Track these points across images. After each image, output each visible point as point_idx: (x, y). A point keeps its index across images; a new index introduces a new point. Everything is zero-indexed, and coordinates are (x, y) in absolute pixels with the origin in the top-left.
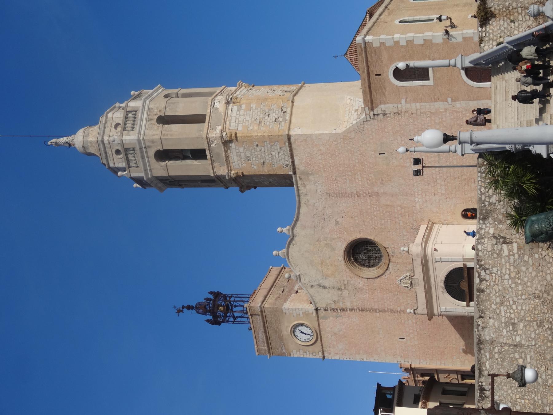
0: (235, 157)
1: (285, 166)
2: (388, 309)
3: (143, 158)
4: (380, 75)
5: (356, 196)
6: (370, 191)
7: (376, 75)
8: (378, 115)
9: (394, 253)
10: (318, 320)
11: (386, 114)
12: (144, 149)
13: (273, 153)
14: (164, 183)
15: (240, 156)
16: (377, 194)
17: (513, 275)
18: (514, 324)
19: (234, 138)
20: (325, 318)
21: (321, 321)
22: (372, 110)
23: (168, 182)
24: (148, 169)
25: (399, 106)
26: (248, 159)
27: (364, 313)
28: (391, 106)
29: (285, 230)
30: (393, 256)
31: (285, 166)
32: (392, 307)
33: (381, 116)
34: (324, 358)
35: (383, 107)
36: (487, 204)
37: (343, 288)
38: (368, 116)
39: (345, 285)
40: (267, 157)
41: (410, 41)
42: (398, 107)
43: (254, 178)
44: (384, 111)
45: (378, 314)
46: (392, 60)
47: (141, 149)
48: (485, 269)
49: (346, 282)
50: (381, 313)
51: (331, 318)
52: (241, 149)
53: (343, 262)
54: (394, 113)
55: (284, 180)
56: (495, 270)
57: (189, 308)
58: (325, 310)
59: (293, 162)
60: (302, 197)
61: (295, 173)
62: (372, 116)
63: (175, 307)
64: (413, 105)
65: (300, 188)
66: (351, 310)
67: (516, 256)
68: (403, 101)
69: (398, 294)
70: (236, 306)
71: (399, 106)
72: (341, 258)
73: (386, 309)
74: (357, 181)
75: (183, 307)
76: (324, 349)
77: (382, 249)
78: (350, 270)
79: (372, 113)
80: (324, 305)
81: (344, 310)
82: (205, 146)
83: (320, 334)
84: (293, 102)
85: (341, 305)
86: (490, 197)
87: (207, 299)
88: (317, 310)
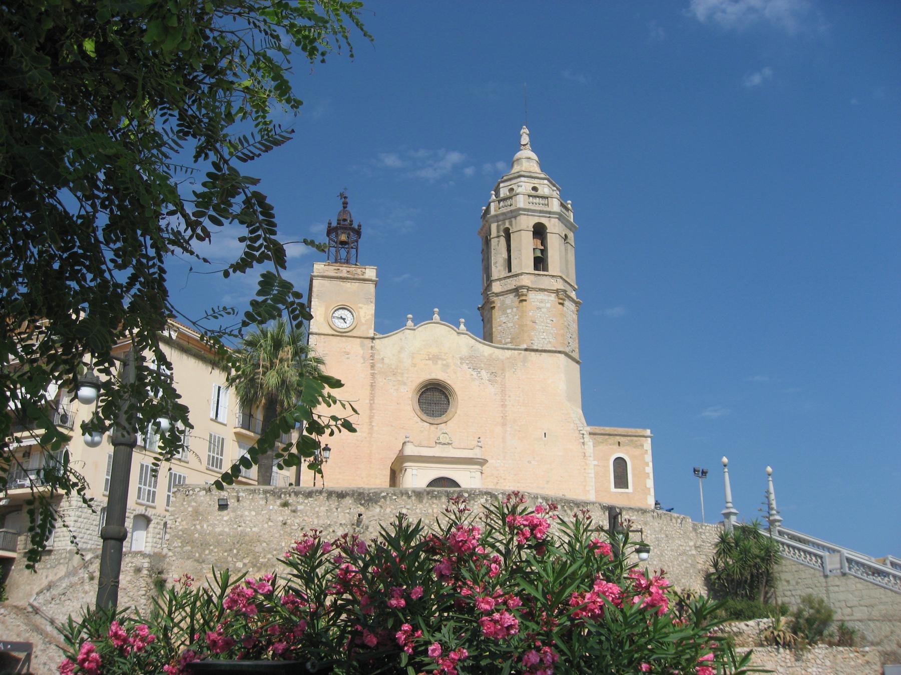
0: (541, 297)
3: (541, 212)
6: (508, 418)
8: (583, 438)
10: (360, 338)
13: (544, 334)
15: (541, 302)
16: (504, 425)
17: (681, 548)
18: (658, 545)
19: (561, 301)
20: (362, 346)
21: (358, 340)
22: (590, 434)
23: (507, 225)
26: (539, 308)
27: (369, 388)
28: (591, 451)
29: (462, 327)
33: (582, 441)
34: (312, 334)
35: (591, 444)
36: (701, 530)
39: (403, 374)
40: (540, 327)
43: (515, 310)
45: (368, 401)
46: (631, 458)
47: (550, 213)
48: (681, 523)
49: (406, 375)
51: (362, 352)
52: (548, 305)
53: (430, 378)
56: (682, 532)
57: (345, 205)
58: (372, 347)
61: (526, 350)
62: (581, 432)
64: (593, 471)
66: (373, 375)
67: (690, 553)
68: (596, 463)
71: (592, 459)
76: (322, 336)
77: (444, 418)
80: (377, 347)
81: (373, 366)
82: (551, 272)
83: (341, 336)
84: (578, 362)
85: (379, 365)
86: (704, 533)
87: (360, 226)
88: (373, 339)
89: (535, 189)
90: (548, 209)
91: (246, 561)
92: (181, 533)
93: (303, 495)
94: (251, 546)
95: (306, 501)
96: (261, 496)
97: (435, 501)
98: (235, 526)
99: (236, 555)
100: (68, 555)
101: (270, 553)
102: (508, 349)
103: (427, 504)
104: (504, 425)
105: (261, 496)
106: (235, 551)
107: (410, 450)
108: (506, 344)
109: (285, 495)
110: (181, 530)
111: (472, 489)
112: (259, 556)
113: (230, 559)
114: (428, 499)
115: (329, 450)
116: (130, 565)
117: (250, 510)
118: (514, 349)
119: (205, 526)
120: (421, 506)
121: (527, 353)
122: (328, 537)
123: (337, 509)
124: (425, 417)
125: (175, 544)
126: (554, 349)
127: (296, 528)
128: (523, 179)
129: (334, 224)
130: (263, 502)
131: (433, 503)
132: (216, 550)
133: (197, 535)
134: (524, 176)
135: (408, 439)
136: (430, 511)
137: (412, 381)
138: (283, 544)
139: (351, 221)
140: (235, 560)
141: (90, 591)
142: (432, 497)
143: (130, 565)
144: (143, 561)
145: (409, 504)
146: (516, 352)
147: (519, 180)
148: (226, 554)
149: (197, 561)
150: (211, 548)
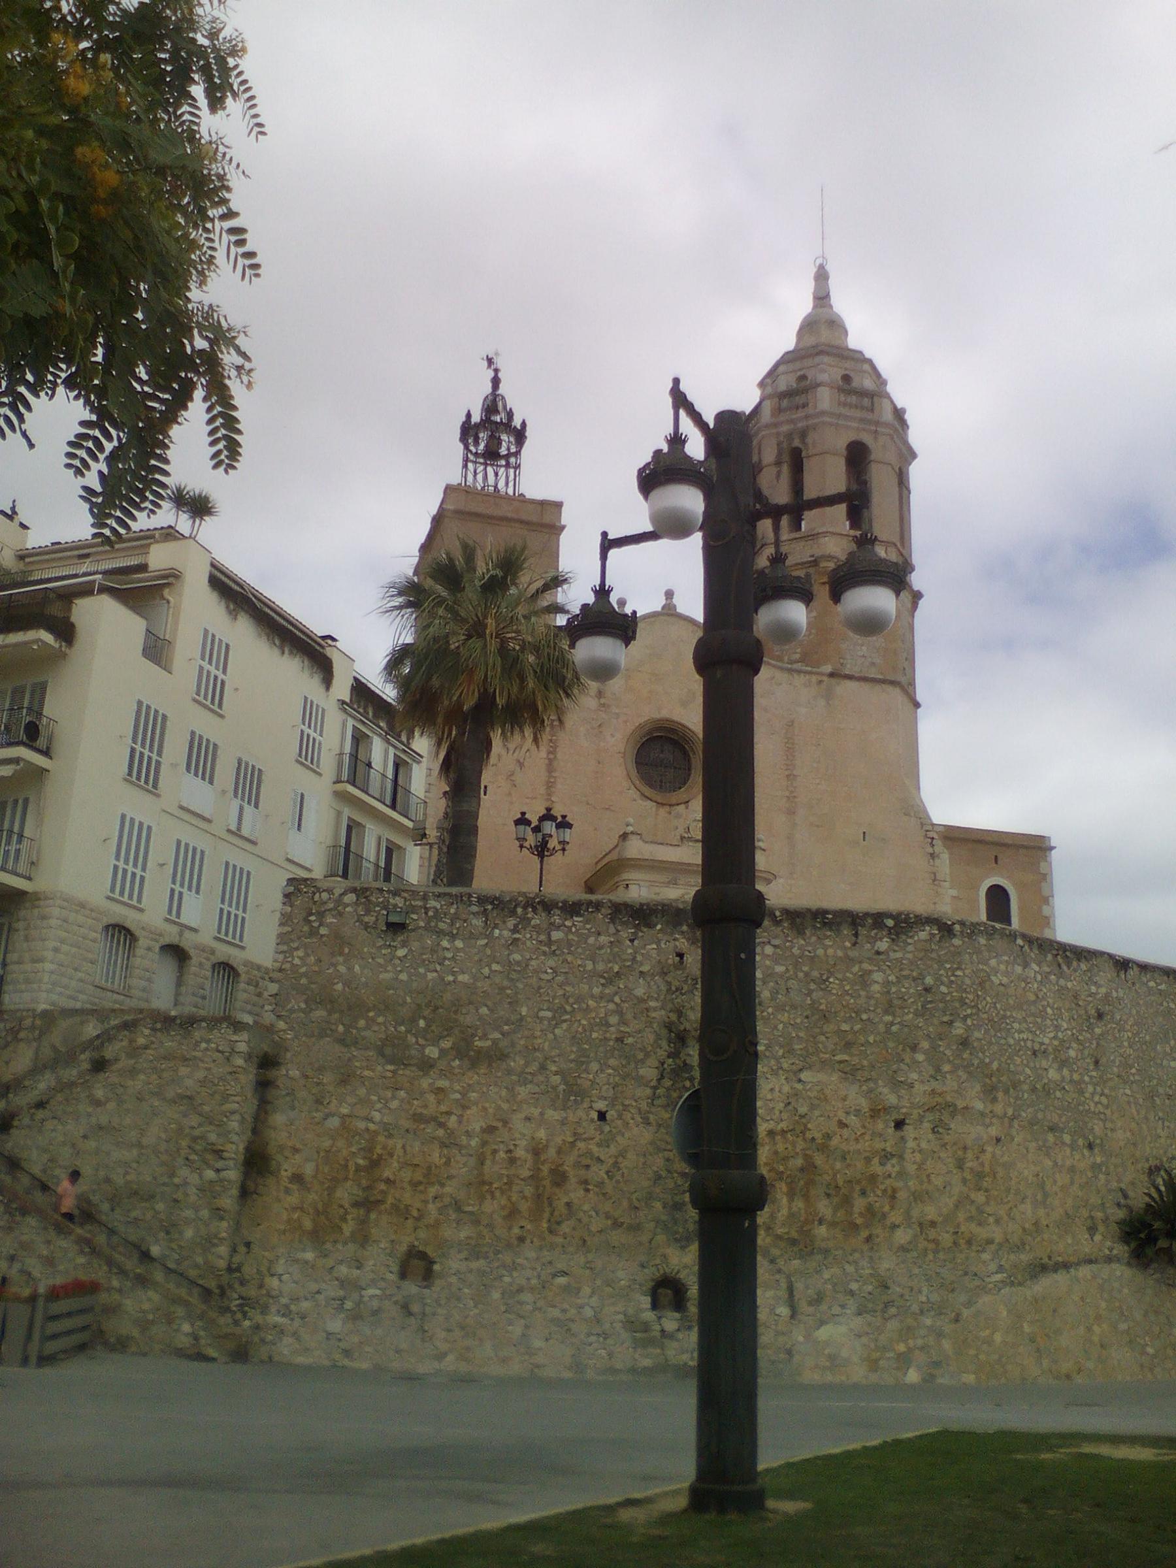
1: (842, 661)
2: (555, 777)
3: (862, 420)
4: (996, 862)
5: (787, 773)
6: (796, 800)
7: (996, 857)
9: (678, 816)
11: (933, 859)
12: (873, 428)
14: (789, 436)
16: (791, 812)
23: (797, 443)
24: (849, 424)
25: (947, 884)
30: (670, 813)
31: (842, 661)
32: (559, 786)
33: (930, 850)
35: (945, 856)
37: (603, 701)
38: (930, 828)
39: (609, 706)
41: (1049, 923)
42: (945, 881)
44: (938, 856)
49: (615, 710)
50: (547, 761)
53: (657, 715)
54: (935, 874)
55: (799, 650)
57: (496, 382)
59: (850, 677)
60: (786, 675)
62: (931, 834)
63: (497, 354)
65: (802, 675)
68: (954, 892)
69: (588, 804)
70: (496, 474)
71: (947, 884)
72: (665, 714)
73: (553, 774)
74: (818, 781)
75: (496, 371)
78: (641, 726)
79: (935, 836)
87: (524, 424)
89: (847, 378)
90: (870, 416)
91: (446, 1044)
92: (304, 981)
93: (561, 908)
94: (456, 1012)
95: (568, 923)
96: (475, 909)
97: (829, 933)
98: (421, 970)
99: (426, 1030)
100: (38, 1022)
101: (497, 1028)
102: (799, 672)
103: (814, 939)
104: (791, 812)
105: (475, 909)
106: (422, 1023)
107: (635, 849)
108: (791, 662)
109: (525, 908)
110: (305, 975)
111: (900, 914)
112: (474, 1035)
113: (411, 1039)
114: (814, 927)
115: (570, 826)
116: (204, 1045)
117: (453, 937)
118: (810, 673)
119: (357, 968)
120: (802, 942)
121: (833, 681)
122: (617, 999)
123: (632, 941)
124: (647, 791)
125: (292, 1004)
126: (880, 677)
127: (549, 977)
128: (826, 359)
129: (476, 418)
130: (478, 922)
131: (827, 937)
132: (380, 1019)
133: (339, 987)
134: (828, 354)
135: (630, 829)
136: (820, 952)
137: (625, 722)
138: (524, 1011)
139: (510, 415)
140: (421, 1041)
141: (108, 1100)
142: (825, 924)
143: (204, 1045)
144: (235, 1038)
145: (776, 937)
146: (814, 678)
147: (817, 359)
148: (403, 1028)
149: (342, 1041)
150: (371, 1014)
